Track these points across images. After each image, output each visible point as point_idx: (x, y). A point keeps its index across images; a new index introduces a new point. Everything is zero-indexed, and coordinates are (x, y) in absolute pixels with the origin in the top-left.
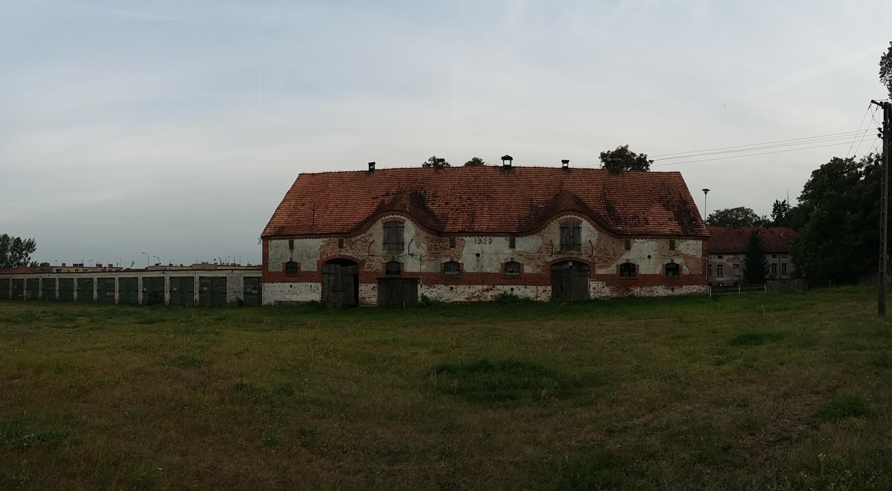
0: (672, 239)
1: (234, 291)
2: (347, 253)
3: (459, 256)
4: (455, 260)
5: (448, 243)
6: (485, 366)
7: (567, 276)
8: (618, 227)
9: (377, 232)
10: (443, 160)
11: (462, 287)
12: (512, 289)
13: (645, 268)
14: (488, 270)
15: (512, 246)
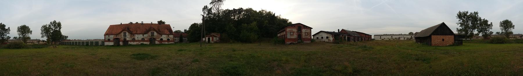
0: (168, 35)
1: (100, 43)
2: (117, 37)
6: (139, 54)
7: (152, 40)
8: (160, 33)
9: (122, 34)
13: (164, 39)
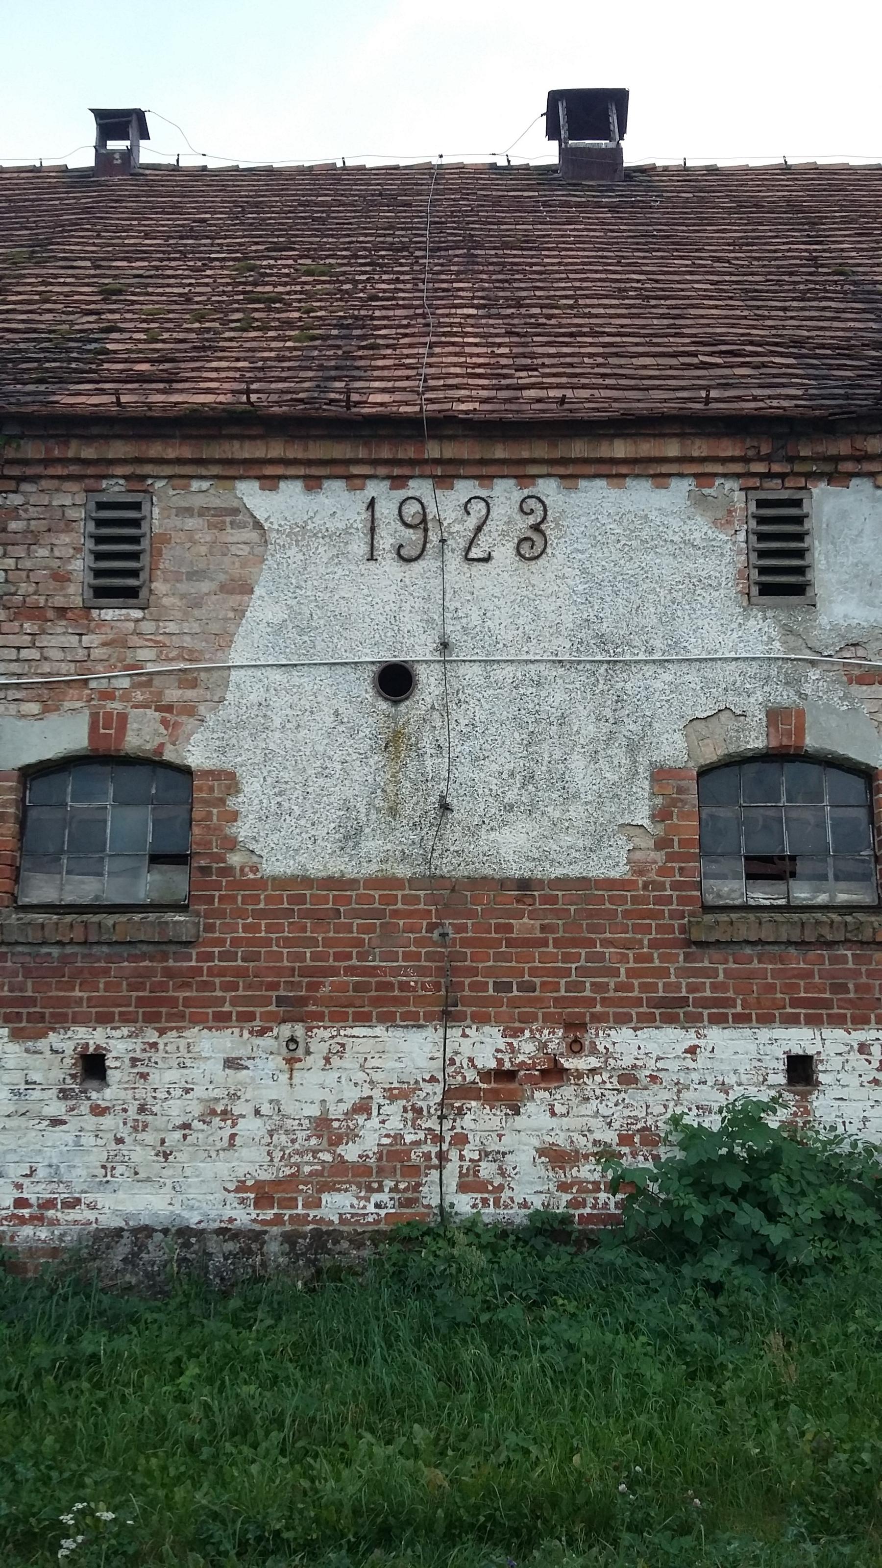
3: (196, 682)
4: (142, 734)
5: (71, 555)
10: (145, 135)
11: (212, 1044)
12: (801, 1070)
14: (511, 847)
15: (780, 572)
